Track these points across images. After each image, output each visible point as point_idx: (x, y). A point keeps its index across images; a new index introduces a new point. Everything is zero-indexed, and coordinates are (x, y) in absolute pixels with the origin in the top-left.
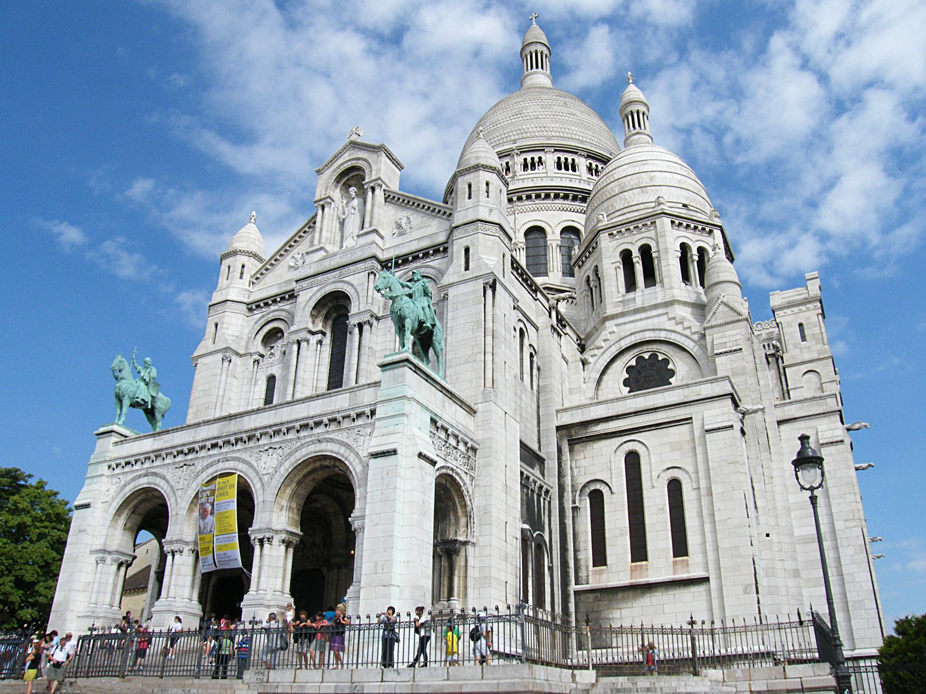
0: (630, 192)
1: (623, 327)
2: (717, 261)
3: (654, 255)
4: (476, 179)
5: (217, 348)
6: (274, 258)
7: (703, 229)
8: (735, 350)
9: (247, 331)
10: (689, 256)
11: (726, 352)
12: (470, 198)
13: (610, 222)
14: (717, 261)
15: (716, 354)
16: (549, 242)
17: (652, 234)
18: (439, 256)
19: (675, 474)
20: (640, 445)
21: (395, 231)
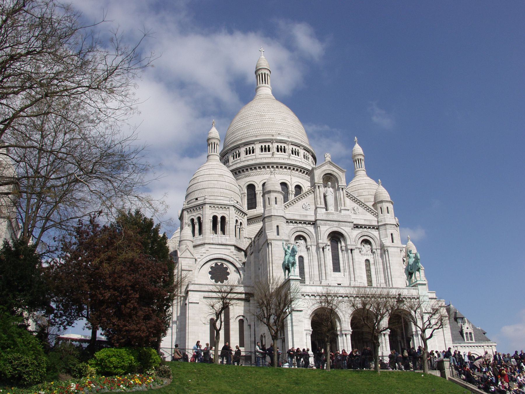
5: (281, 238)
12: (388, 213)
21: (353, 211)
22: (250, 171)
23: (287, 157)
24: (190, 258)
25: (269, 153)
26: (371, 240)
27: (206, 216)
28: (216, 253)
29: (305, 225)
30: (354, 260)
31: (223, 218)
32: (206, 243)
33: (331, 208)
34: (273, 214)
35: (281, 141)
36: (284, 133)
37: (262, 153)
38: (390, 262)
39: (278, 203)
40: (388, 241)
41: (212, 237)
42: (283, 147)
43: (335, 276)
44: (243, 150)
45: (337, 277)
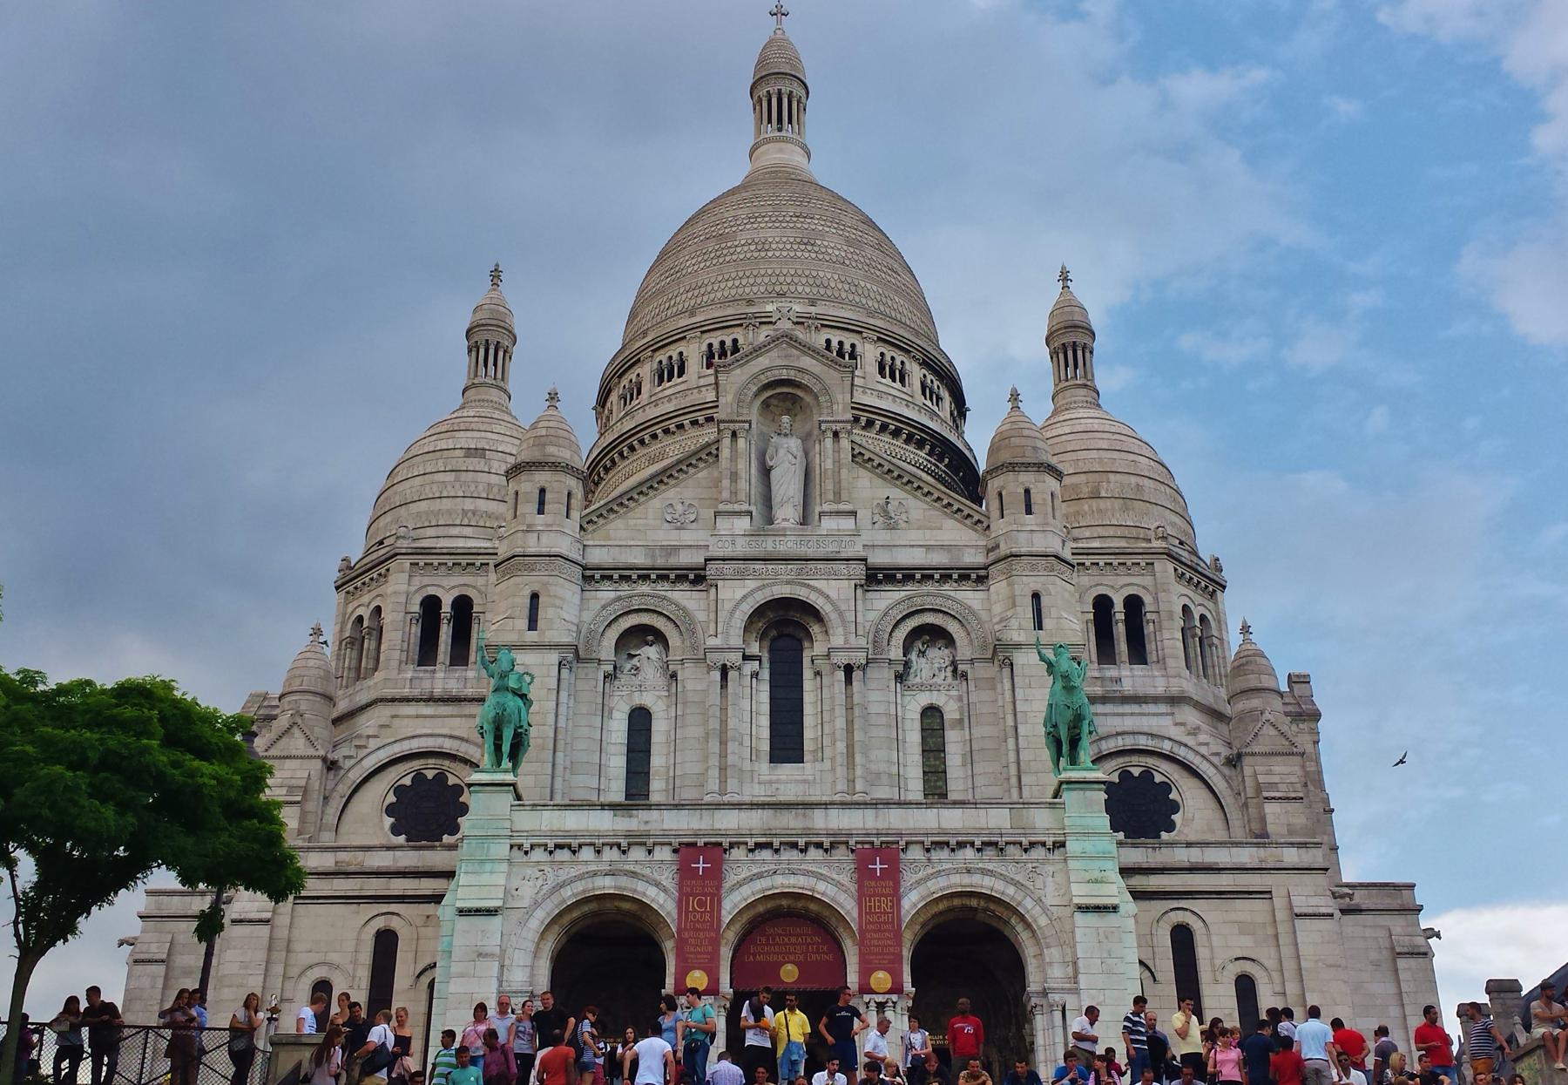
0: (1108, 503)
2: (1254, 655)
3: (1149, 616)
4: (1039, 485)
6: (629, 496)
7: (1207, 587)
8: (1295, 798)
9: (587, 616)
11: (1280, 798)
13: (1080, 545)
14: (1254, 655)
15: (1267, 798)
17: (1147, 580)
18: (966, 585)
19: (1248, 967)
20: (1195, 917)
24: (302, 758)
26: (952, 627)
28: (419, 732)
29: (663, 588)
31: (463, 606)
33: (786, 514)
34: (519, 551)
36: (800, 289)
38: (1019, 708)
40: (1014, 623)
41: (409, 675)
43: (774, 778)
44: (646, 371)
45: (778, 782)
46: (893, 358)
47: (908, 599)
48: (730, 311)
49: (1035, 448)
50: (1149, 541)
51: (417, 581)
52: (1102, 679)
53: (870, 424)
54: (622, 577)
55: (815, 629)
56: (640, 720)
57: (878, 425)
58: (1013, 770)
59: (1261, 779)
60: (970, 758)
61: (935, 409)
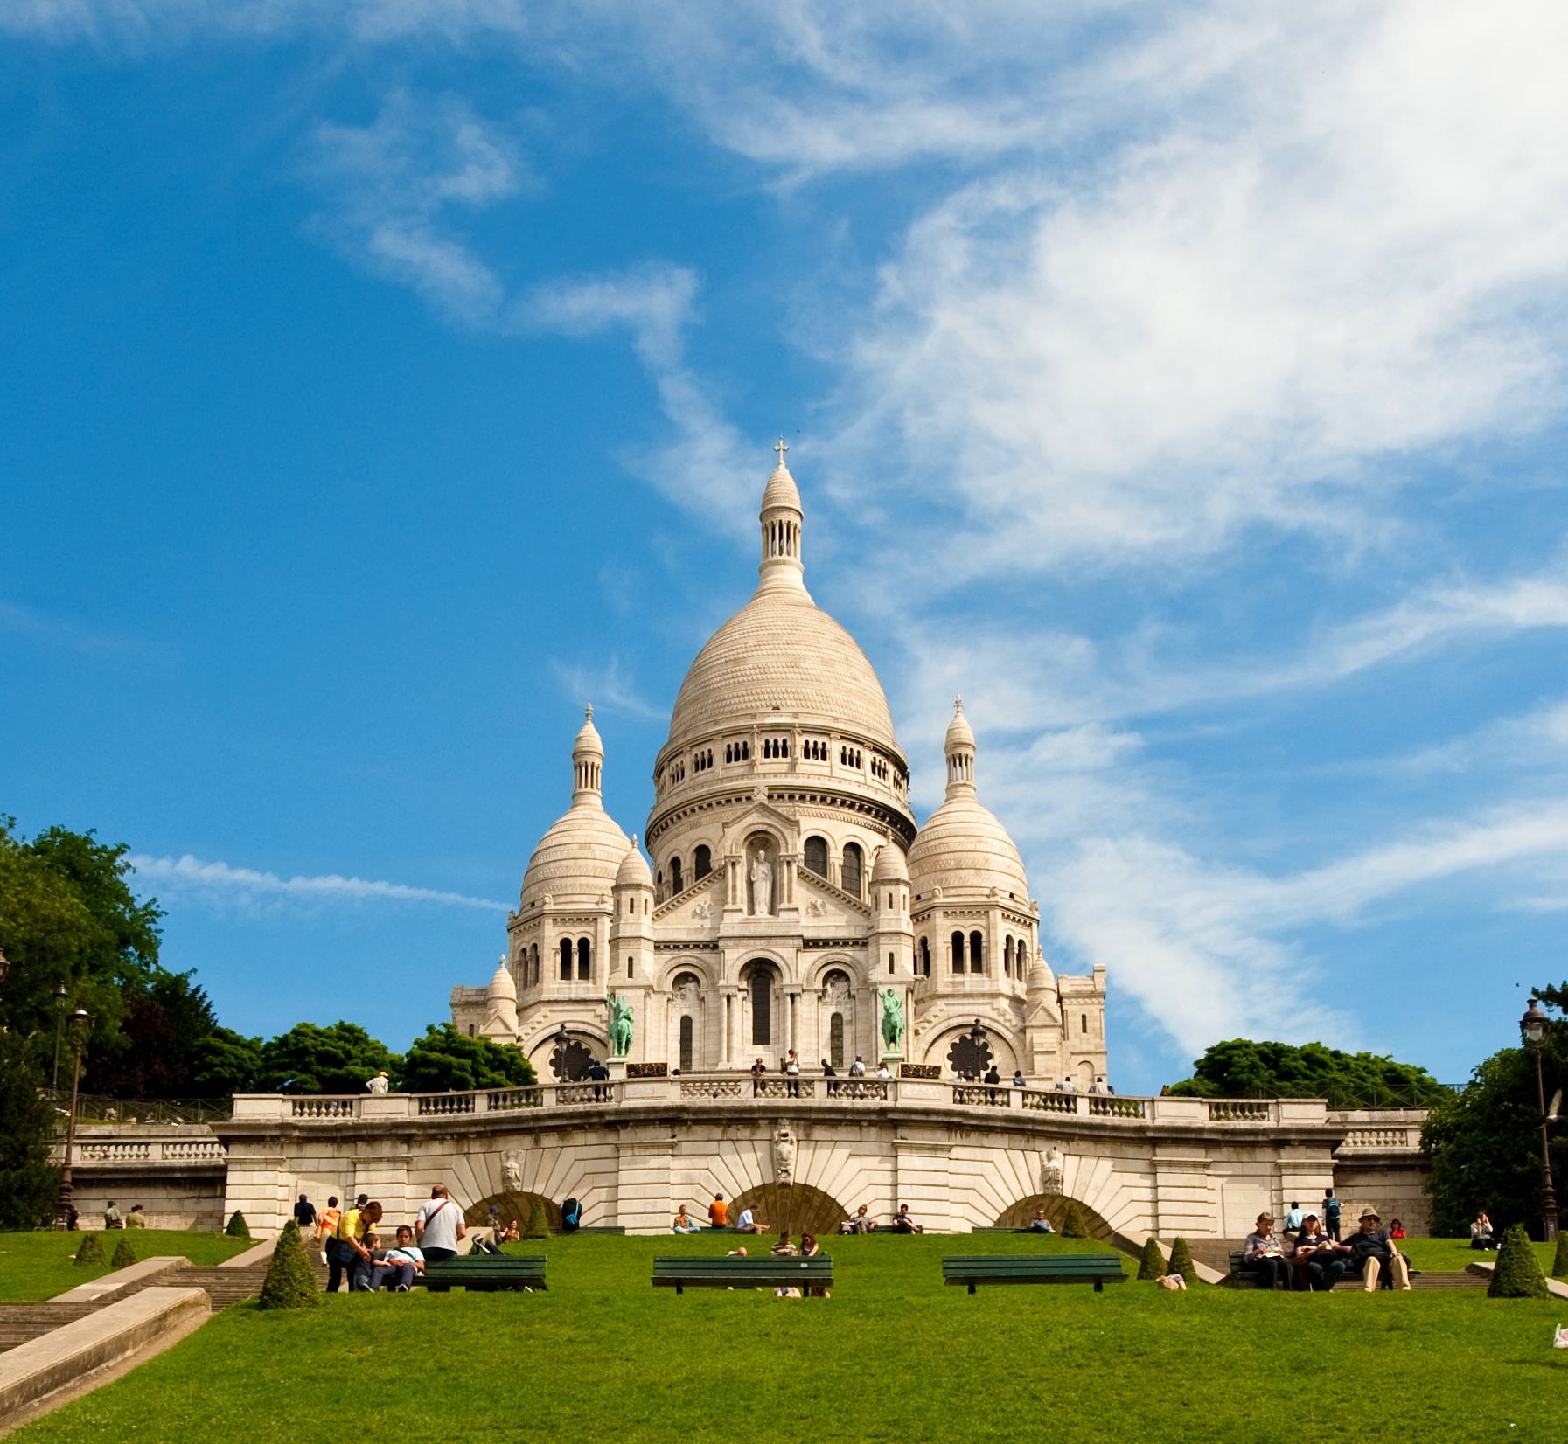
1: (951, 1008)
3: (984, 944)
7: (1025, 922)
10: (1010, 947)
12: (891, 907)
16: (831, 860)
17: (983, 922)
18: (857, 948)
22: (700, 814)
23: (786, 766)
25: (745, 762)
26: (849, 971)
27: (546, 940)
29: (696, 953)
30: (798, 1019)
31: (584, 943)
32: (540, 1002)
34: (620, 935)
35: (776, 728)
36: (789, 702)
37: (729, 765)
39: (635, 910)
41: (556, 986)
42: (780, 743)
44: (687, 760)
46: (851, 750)
47: (826, 955)
48: (742, 723)
49: (896, 870)
50: (988, 896)
51: (557, 930)
52: (953, 983)
53: (833, 801)
54: (675, 947)
55: (776, 974)
56: (686, 1023)
57: (839, 801)
58: (874, 1048)
59: (1034, 1041)
60: (855, 1040)
61: (882, 780)
